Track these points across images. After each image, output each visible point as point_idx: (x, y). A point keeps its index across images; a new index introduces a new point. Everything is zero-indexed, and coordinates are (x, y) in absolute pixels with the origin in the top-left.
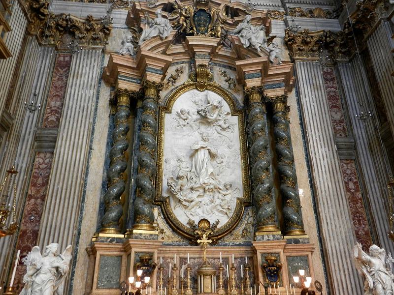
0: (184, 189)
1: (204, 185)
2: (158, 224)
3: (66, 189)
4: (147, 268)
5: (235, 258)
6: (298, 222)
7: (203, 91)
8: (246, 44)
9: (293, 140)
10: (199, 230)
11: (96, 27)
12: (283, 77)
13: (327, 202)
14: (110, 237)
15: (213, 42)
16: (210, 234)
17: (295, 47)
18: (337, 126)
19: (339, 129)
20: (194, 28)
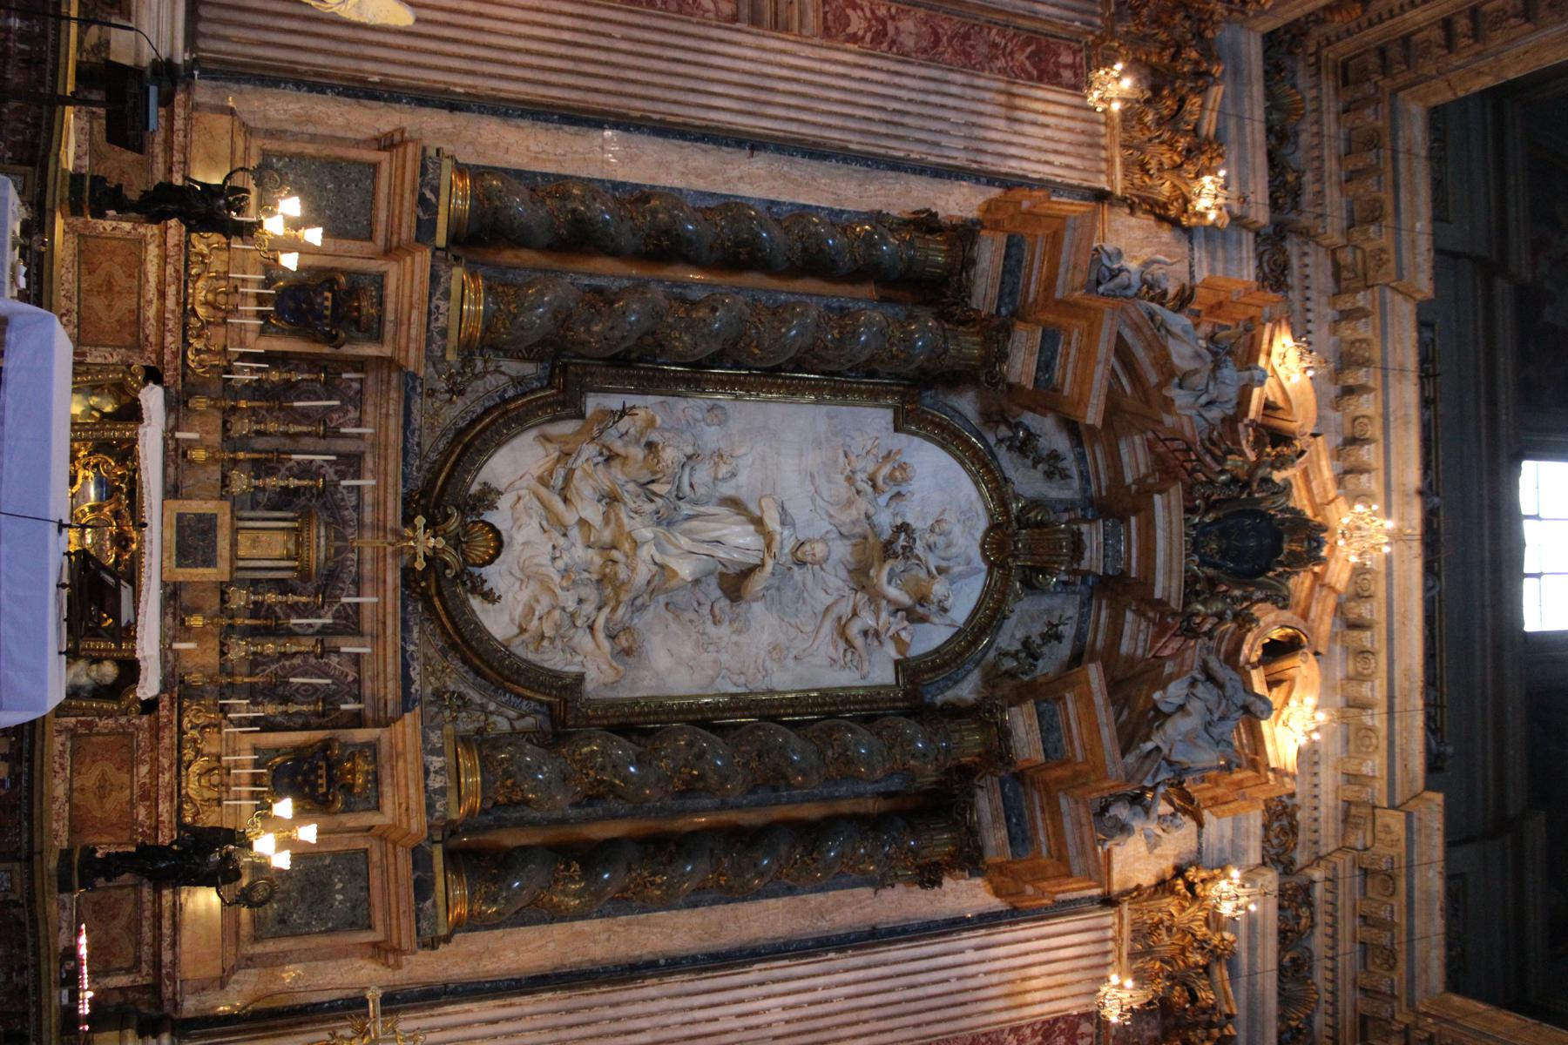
0: (613, 471)
1: (627, 546)
4: (328, 313)
5: (357, 659)
9: (813, 904)
10: (464, 525)
13: (577, 1025)
14: (437, 197)
15: (1167, 585)
16: (447, 565)
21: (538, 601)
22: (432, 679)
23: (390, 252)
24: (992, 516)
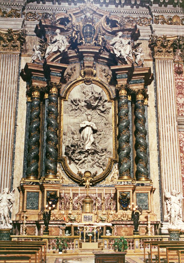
3: (3, 152)
8: (118, 54)
10: (84, 177)
16: (91, 180)
17: (156, 49)
18: (180, 108)
19: (182, 110)
20: (84, 39)
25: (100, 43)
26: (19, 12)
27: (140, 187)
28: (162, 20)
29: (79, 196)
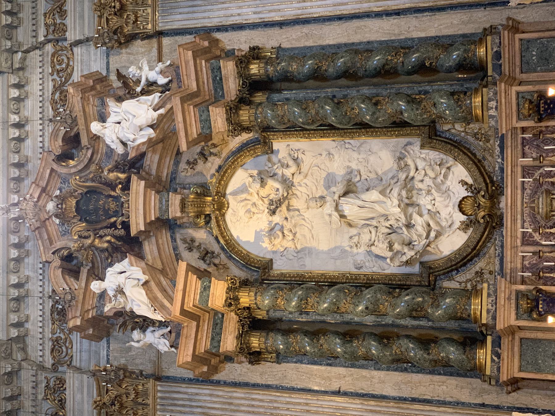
1: (402, 205)
2: (468, 281)
4: (541, 302)
5: (524, 155)
6: (465, 50)
7: (228, 204)
10: (476, 215)
11: (113, 393)
12: (201, 63)
14: (492, 358)
20: (113, 220)
21: (442, 181)
22: (490, 146)
23: (512, 331)
24: (224, 220)
25: (122, 176)
26: (52, 380)
27: (505, 62)
28: (57, 16)
29: (530, 230)
